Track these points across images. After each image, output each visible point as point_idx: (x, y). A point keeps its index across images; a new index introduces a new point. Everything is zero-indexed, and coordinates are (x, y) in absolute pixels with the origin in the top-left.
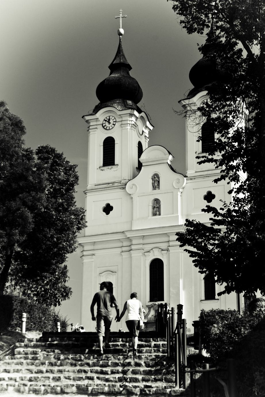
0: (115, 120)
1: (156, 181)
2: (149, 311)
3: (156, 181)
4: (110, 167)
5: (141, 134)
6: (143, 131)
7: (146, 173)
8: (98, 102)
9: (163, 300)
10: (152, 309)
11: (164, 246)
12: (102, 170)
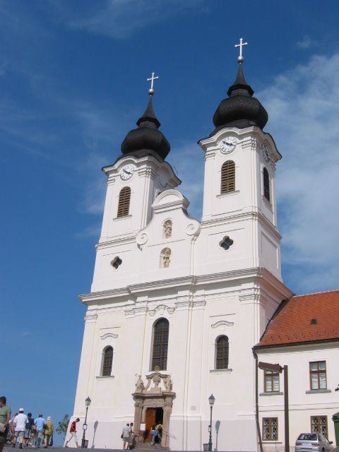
2: (149, 383)
6: (167, 184)
7: (159, 219)
8: (122, 154)
9: (166, 369)
10: (152, 380)
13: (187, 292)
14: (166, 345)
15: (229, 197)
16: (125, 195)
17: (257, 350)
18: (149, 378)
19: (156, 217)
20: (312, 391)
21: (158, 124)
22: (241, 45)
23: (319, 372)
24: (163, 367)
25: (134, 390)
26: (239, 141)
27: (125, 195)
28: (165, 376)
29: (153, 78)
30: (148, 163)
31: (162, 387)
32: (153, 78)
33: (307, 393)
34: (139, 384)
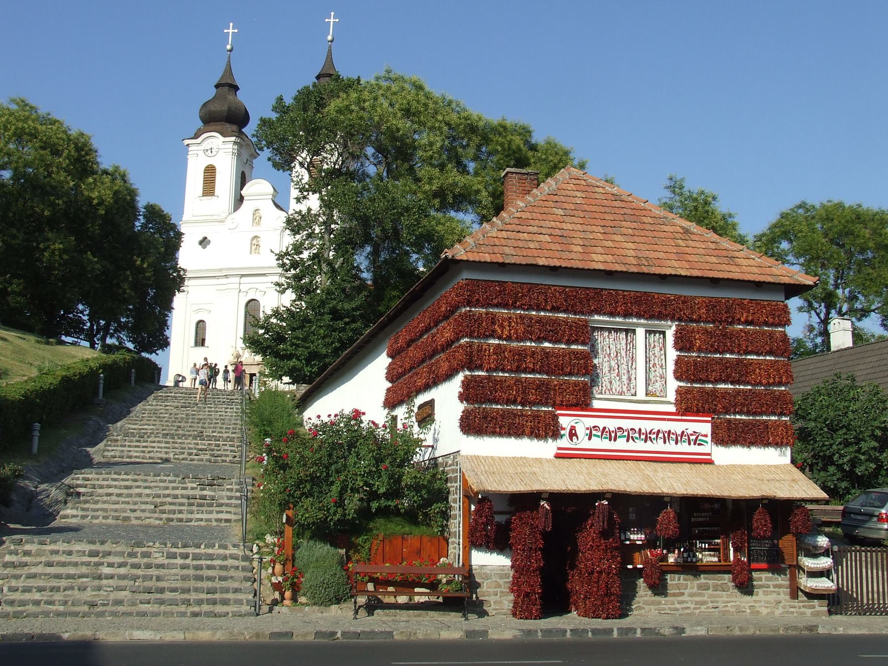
1: (257, 217)
2: (244, 353)
4: (210, 198)
11: (262, 287)
16: (210, 172)
21: (236, 88)
22: (332, 20)
27: (210, 172)
29: (231, 31)
30: (235, 143)
32: (231, 31)
34: (235, 355)
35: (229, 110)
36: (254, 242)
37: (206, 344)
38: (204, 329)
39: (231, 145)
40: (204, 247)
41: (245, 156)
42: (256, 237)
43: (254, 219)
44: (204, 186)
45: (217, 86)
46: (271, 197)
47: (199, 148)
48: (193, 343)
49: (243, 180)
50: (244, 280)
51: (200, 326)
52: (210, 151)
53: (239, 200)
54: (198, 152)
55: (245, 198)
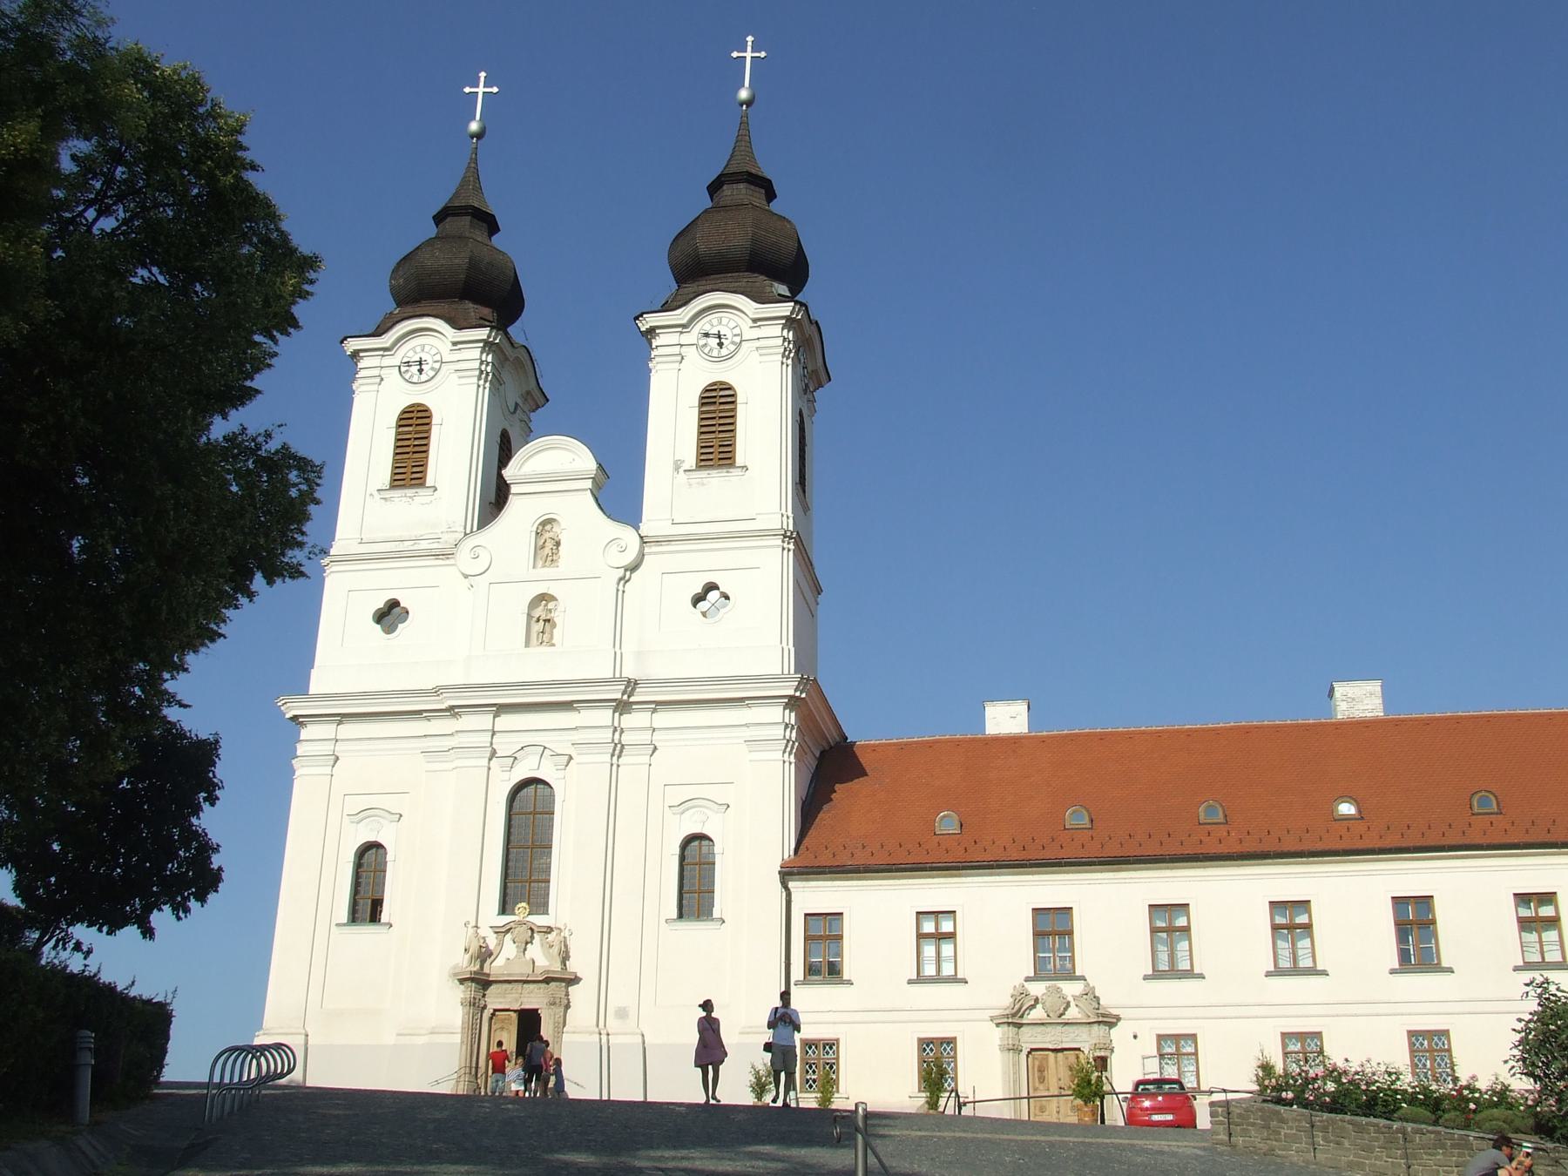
0: (438, 358)
2: (501, 944)
3: (549, 541)
4: (410, 492)
5: (512, 410)
6: (517, 404)
8: (390, 305)
9: (546, 912)
10: (509, 936)
11: (560, 744)
12: (385, 499)
13: (605, 716)
14: (543, 846)
15: (716, 479)
17: (788, 874)
18: (501, 932)
19: (514, 505)
20: (920, 979)
21: (492, 226)
22: (749, 55)
23: (940, 937)
24: (541, 906)
25: (463, 963)
26: (750, 333)
28: (549, 930)
29: (481, 90)
30: (488, 345)
31: (541, 957)
32: (481, 90)
33: (910, 982)
34: (474, 949)
35: (473, 264)
36: (538, 612)
37: (384, 917)
38: (381, 870)
39: (475, 353)
40: (390, 629)
41: (513, 395)
42: (543, 598)
43: (539, 548)
44: (395, 461)
45: (439, 218)
46: (589, 484)
47: (387, 361)
48: (343, 914)
49: (503, 449)
50: (506, 721)
51: (370, 859)
52: (415, 369)
53: (496, 497)
54: (384, 372)
55: (514, 489)
